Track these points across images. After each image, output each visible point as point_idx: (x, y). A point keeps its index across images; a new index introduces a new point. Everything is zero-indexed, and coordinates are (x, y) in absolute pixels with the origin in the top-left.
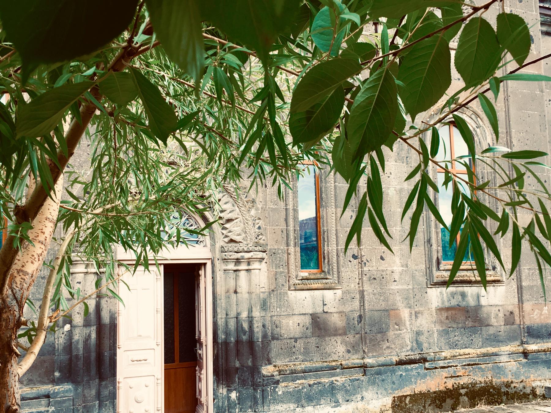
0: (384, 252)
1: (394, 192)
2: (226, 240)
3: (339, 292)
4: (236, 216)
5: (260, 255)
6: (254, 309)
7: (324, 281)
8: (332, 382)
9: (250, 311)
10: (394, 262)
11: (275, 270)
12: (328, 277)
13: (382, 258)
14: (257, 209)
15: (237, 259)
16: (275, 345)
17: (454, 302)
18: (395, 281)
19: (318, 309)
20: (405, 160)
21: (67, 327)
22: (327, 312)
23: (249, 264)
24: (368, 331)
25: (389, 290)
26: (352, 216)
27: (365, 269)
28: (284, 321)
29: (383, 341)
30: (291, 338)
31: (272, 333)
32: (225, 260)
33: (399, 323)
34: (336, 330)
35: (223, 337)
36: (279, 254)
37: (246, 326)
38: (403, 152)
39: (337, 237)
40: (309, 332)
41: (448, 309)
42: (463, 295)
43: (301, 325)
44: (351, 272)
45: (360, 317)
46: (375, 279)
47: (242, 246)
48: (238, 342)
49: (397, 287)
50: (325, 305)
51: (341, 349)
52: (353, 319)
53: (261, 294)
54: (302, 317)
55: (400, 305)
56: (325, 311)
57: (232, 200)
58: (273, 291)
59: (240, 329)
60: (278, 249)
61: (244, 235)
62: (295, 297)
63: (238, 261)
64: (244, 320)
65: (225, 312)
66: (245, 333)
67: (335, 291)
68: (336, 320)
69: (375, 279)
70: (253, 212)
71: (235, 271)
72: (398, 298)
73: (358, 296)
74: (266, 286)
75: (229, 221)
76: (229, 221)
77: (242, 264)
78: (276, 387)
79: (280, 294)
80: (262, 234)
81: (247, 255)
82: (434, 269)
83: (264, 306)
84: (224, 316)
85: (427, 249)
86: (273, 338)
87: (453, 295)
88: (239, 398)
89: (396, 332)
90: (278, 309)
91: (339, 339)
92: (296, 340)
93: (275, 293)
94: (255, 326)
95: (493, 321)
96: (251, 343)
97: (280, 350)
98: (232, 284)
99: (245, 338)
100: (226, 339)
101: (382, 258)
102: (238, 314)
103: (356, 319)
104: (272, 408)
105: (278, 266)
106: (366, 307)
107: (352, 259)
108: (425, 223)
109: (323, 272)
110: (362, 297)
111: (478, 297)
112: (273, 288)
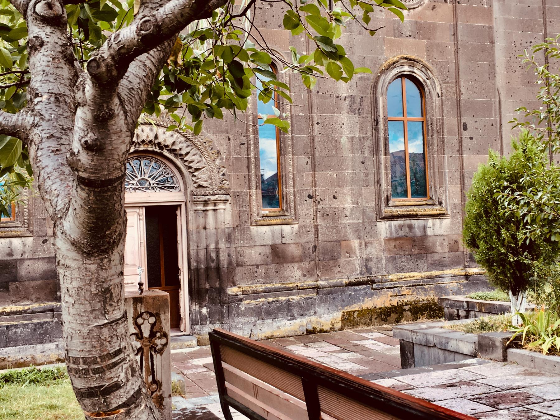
0: (336, 192)
1: (346, 140)
2: (196, 185)
3: (296, 227)
4: (203, 166)
5: (224, 197)
6: (220, 242)
7: (283, 217)
8: (288, 300)
9: (217, 243)
10: (346, 200)
11: (239, 210)
12: (286, 214)
13: (335, 197)
14: (222, 159)
15: (205, 201)
16: (239, 271)
17: (401, 233)
18: (346, 216)
19: (277, 241)
20: (357, 112)
22: (285, 244)
23: (215, 205)
24: (322, 259)
25: (341, 224)
26: (307, 162)
27: (319, 207)
28: (247, 251)
29: (335, 266)
30: (253, 265)
31: (236, 261)
32: (195, 202)
33: (350, 251)
35: (195, 264)
36: (242, 195)
37: (214, 255)
38: (355, 105)
39: (294, 180)
40: (269, 260)
41: (396, 239)
42: (411, 227)
43: (262, 254)
44: (307, 209)
45: (315, 247)
46: (328, 215)
47: (208, 191)
48: (207, 268)
49: (348, 222)
50: (283, 237)
51: (297, 273)
52: (309, 249)
53: (226, 230)
54: (263, 247)
55: (350, 236)
56: (284, 242)
57: (199, 152)
58: (237, 226)
59: (209, 258)
60: (241, 192)
61: (210, 181)
62: (257, 231)
63: (206, 203)
64: (212, 251)
65: (196, 244)
66: (213, 261)
67: (292, 226)
68: (294, 250)
69: (328, 215)
70: (218, 162)
71: (204, 211)
72: (349, 230)
73: (313, 230)
74: (230, 223)
75: (197, 169)
76: (197, 169)
77: (210, 205)
78: (240, 304)
79: (244, 229)
80: (225, 180)
81: (213, 198)
82: (383, 205)
83: (229, 238)
84: (195, 248)
85: (376, 188)
86: (238, 265)
87: (401, 227)
88: (209, 313)
89: (347, 259)
90: (242, 242)
91: (296, 265)
92: (258, 267)
93: (239, 228)
94: (221, 255)
95: (438, 249)
96: (218, 269)
97: (244, 275)
98: (201, 221)
99: (213, 265)
100: (197, 266)
101: (335, 197)
102: (208, 246)
103: (311, 249)
104: (236, 320)
105: (241, 206)
106: (320, 239)
107: (307, 199)
108: (375, 166)
109: (283, 210)
110: (317, 230)
111: (425, 228)
112: (236, 224)
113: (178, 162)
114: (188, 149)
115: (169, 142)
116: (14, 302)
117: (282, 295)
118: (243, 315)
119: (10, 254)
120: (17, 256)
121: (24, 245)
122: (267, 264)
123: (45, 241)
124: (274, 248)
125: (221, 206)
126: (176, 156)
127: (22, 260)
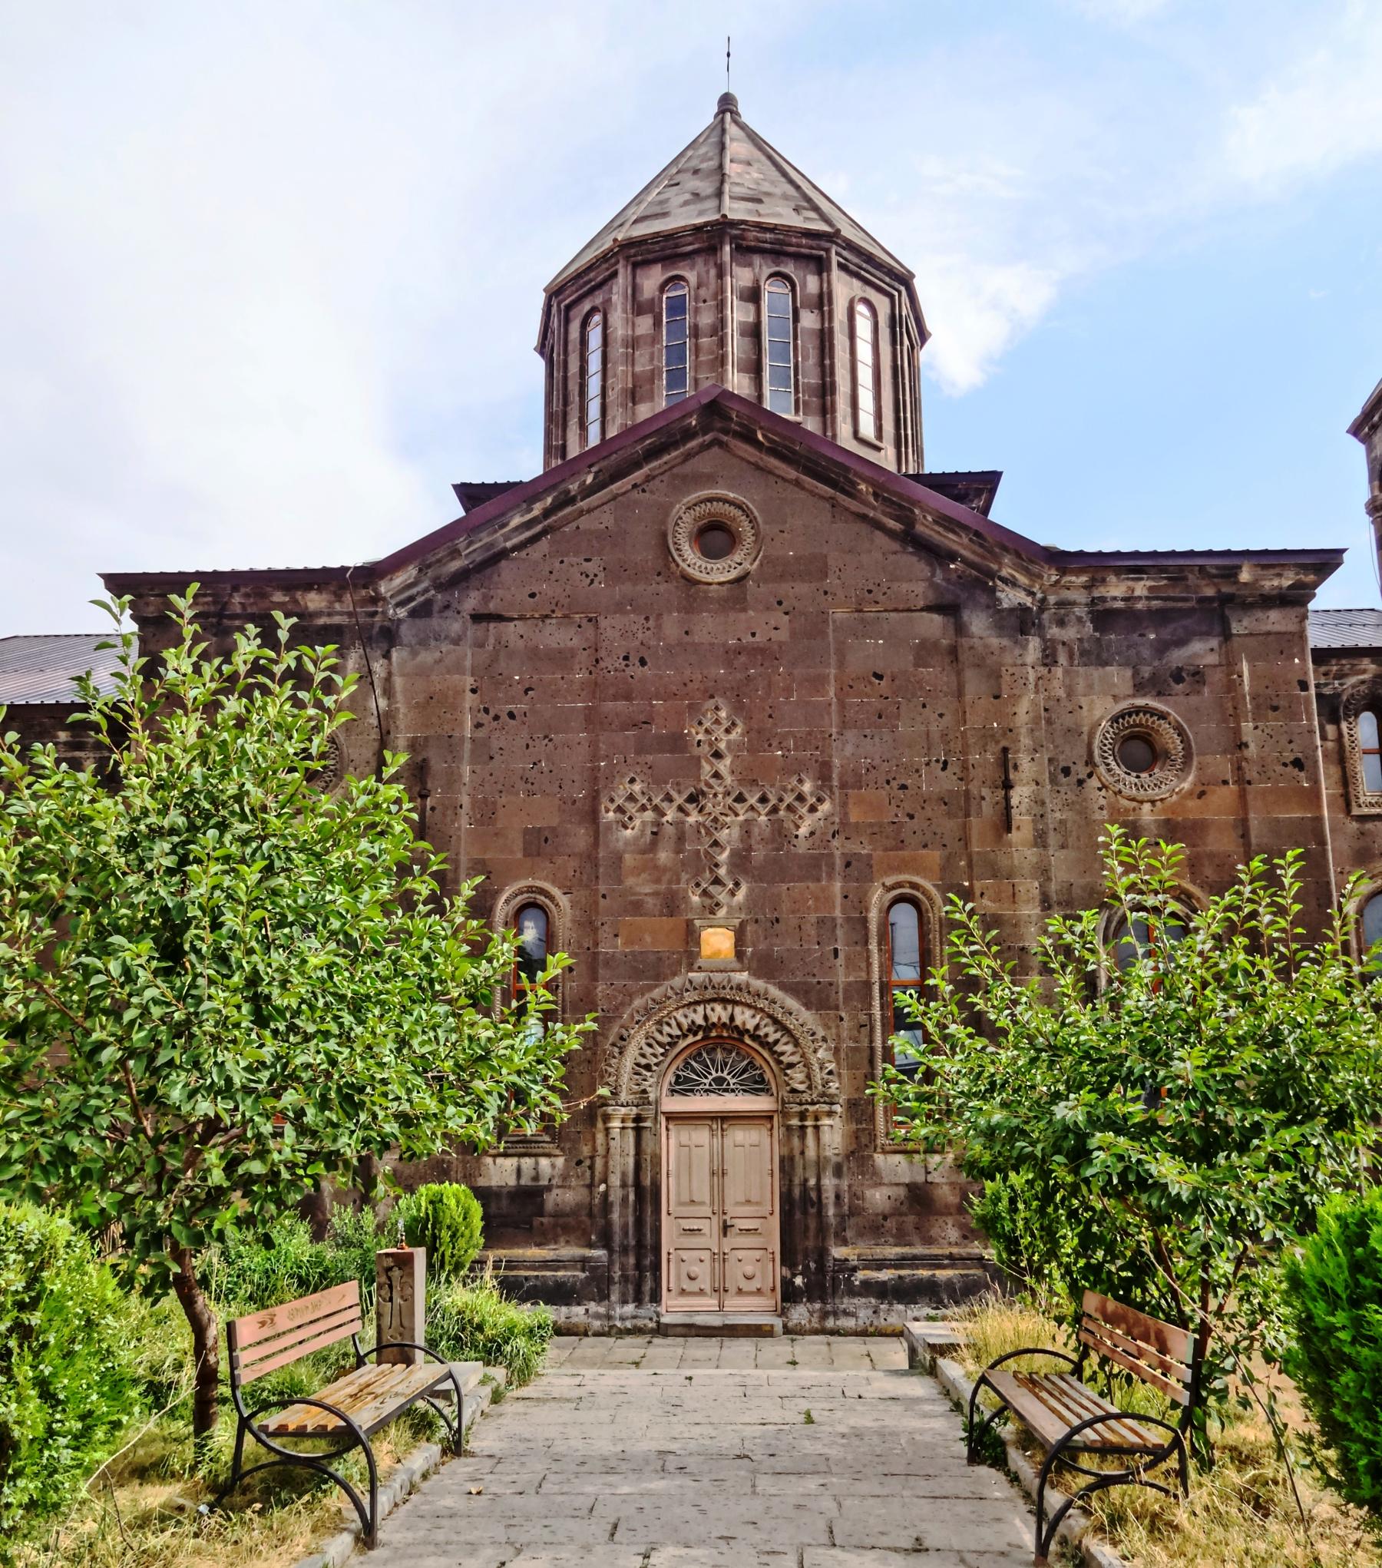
21: (603, 1187)
28: (868, 1193)
34: (947, 1206)
40: (904, 1208)
47: (806, 1097)
81: (811, 1108)
91: (950, 1221)
92: (885, 1218)
102: (806, 1180)
105: (859, 1122)
113: (766, 1054)
114: (778, 1035)
115: (750, 1026)
116: (538, 1245)
117: (924, 1267)
118: (852, 1292)
119: (536, 1178)
120: (544, 1182)
121: (553, 1166)
122: (901, 1214)
123: (579, 1163)
124: (912, 1187)
125: (826, 1121)
126: (762, 1044)
127: (549, 1188)
